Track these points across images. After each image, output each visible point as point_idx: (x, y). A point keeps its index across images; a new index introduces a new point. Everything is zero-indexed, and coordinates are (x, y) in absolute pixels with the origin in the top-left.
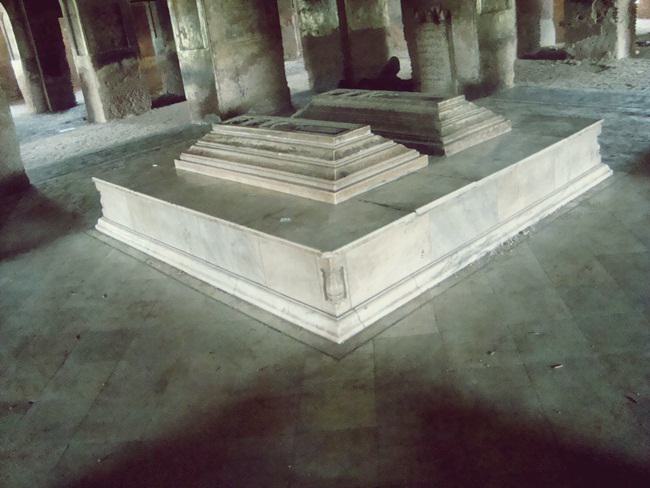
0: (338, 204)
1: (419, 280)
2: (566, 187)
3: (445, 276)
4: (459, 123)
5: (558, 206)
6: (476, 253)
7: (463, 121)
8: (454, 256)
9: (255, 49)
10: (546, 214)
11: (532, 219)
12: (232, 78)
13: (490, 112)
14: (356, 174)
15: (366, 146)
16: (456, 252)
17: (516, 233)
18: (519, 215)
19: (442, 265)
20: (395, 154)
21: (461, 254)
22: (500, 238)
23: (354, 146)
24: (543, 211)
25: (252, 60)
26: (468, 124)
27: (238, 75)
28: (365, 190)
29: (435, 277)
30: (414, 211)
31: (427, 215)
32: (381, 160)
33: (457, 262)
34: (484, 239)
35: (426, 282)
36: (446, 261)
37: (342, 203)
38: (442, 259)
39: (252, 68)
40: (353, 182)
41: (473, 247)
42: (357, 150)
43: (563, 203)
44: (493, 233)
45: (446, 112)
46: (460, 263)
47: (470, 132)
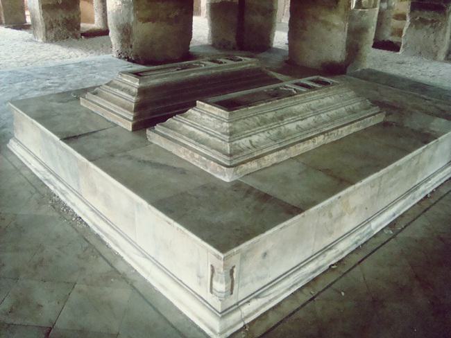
2: (146, 256)
4: (187, 127)
5: (122, 254)
6: (55, 188)
7: (192, 129)
8: (48, 174)
10: (105, 239)
11: (94, 225)
16: (51, 173)
17: (80, 214)
18: (94, 210)
20: (123, 106)
22: (69, 201)
24: (107, 235)
26: (191, 136)
32: (115, 103)
33: (47, 178)
34: (64, 188)
36: (44, 170)
40: (94, 100)
41: (58, 182)
42: (119, 87)
44: (71, 194)
46: (47, 180)
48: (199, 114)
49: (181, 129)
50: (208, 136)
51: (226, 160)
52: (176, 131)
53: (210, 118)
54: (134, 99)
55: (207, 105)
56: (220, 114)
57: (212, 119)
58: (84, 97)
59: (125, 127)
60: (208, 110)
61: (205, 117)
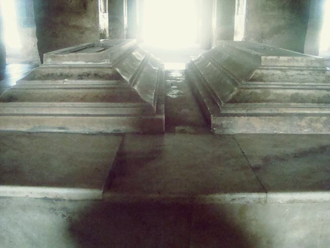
14: (25, 104)
23: (67, 71)
28: (24, 128)
45: (265, 72)
48: (279, 72)
49: (271, 97)
52: (268, 101)
53: (301, 72)
55: (282, 58)
57: (305, 72)
60: (287, 64)
61: (290, 73)
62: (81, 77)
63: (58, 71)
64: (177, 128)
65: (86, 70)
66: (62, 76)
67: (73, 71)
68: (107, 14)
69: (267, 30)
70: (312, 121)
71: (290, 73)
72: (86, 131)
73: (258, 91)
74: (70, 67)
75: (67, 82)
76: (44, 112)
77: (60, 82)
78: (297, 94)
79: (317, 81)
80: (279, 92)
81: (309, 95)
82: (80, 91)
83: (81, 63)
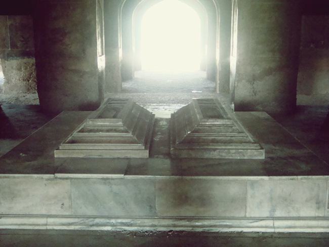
0: (56, 158)
1: (51, 220)
3: (72, 228)
5: (239, 230)
6: (111, 226)
9: (273, 65)
12: (249, 81)
13: (250, 138)
14: (80, 144)
15: (116, 131)
19: (76, 220)
21: (97, 221)
23: (100, 128)
25: (269, 72)
27: (254, 80)
28: (81, 156)
29: (63, 225)
30: (54, 174)
31: (69, 181)
35: (55, 224)
36: (80, 219)
37: (59, 158)
38: (76, 217)
39: (267, 78)
41: (113, 221)
43: (245, 230)
47: (209, 147)
48: (207, 128)
50: (229, 138)
51: (256, 146)
54: (130, 135)
56: (224, 123)
57: (221, 127)
58: (58, 149)
59: (138, 157)
61: (213, 128)
62: (108, 131)
63: (96, 128)
64: (155, 156)
65: (110, 128)
66: (98, 131)
67: (103, 128)
68: (104, 56)
69: (259, 72)
70: (220, 152)
71: (213, 128)
72: (112, 157)
73: (195, 138)
74: (102, 126)
75: (101, 134)
76: (91, 148)
77: (97, 133)
78: (214, 139)
79: (227, 132)
80: (205, 138)
81: (220, 140)
82: (108, 138)
83: (107, 124)
